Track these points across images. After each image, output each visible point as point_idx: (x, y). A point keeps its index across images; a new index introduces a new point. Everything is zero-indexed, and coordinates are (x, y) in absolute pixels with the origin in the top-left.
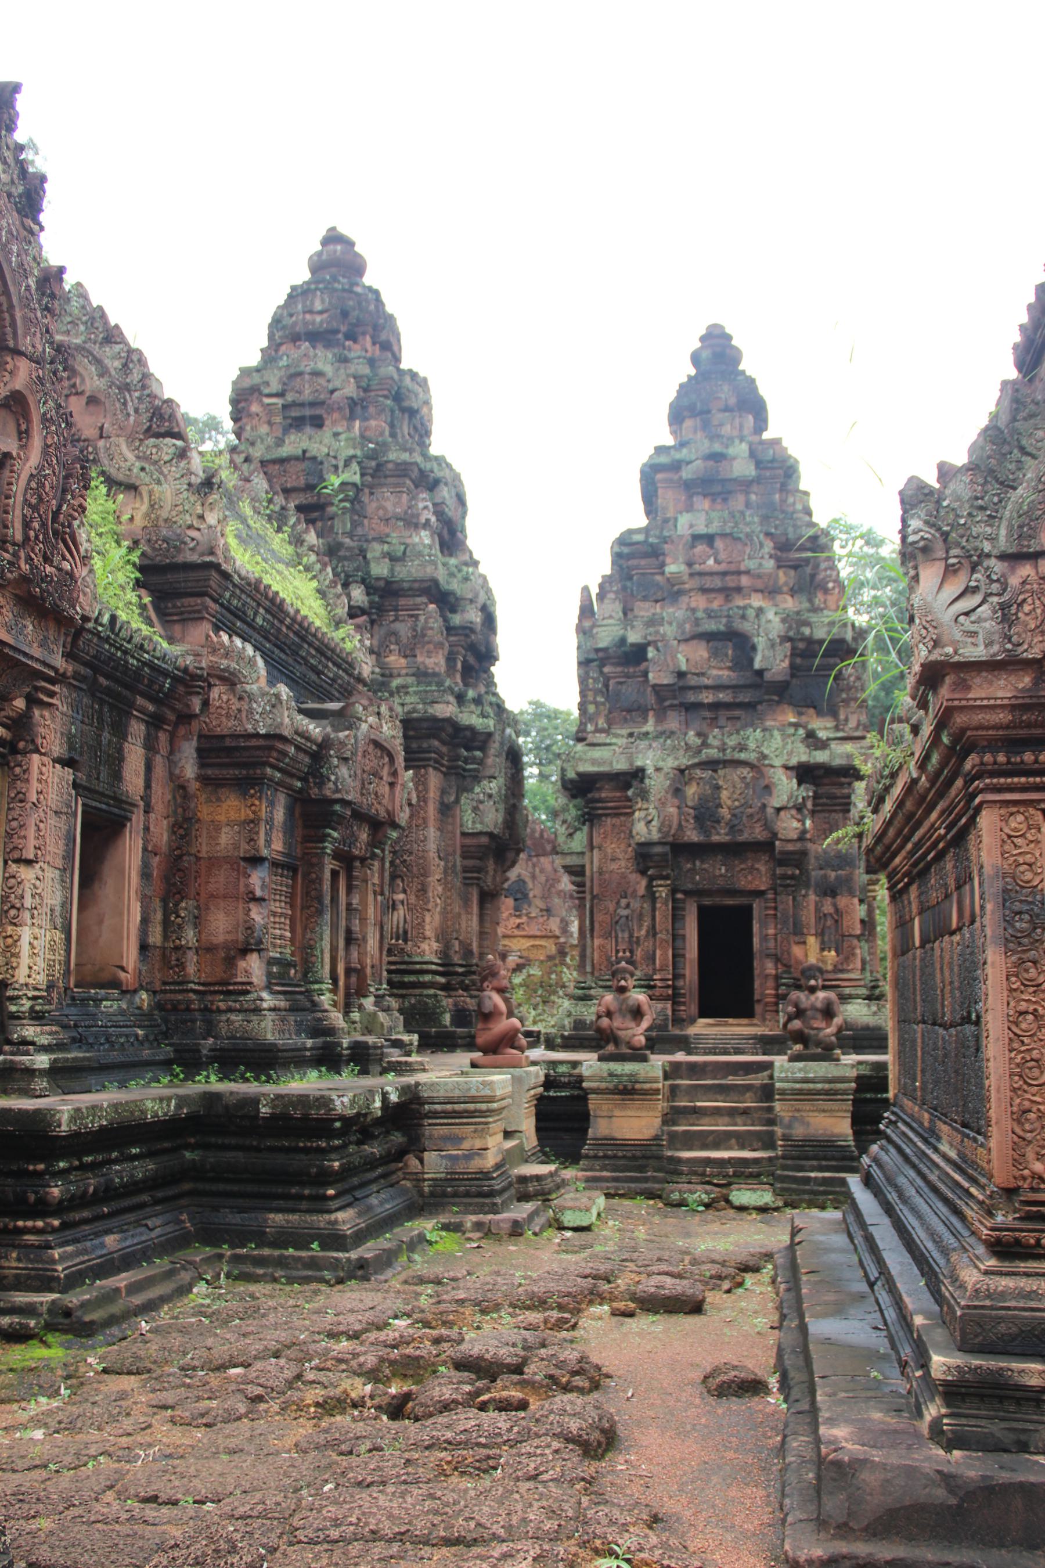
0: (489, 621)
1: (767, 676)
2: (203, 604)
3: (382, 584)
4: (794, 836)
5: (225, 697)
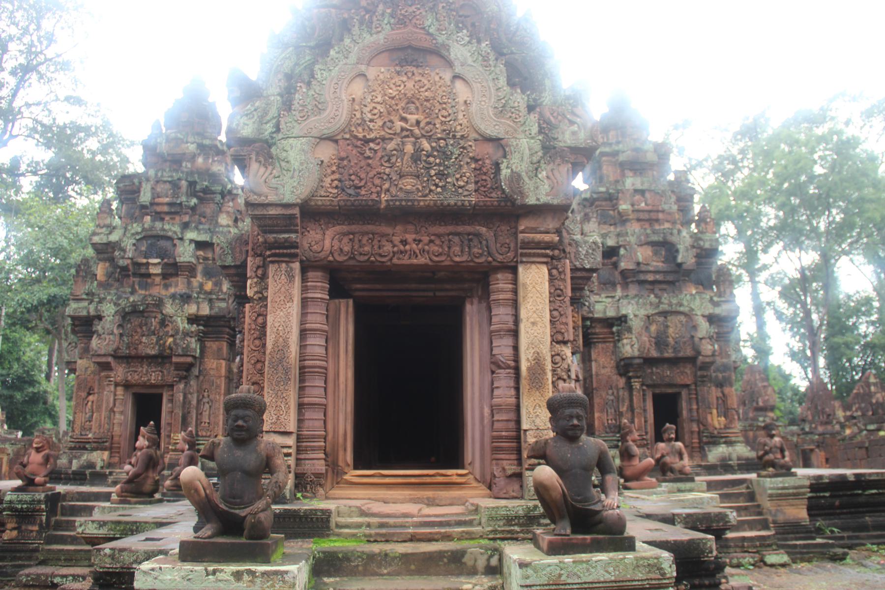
4: (710, 353)
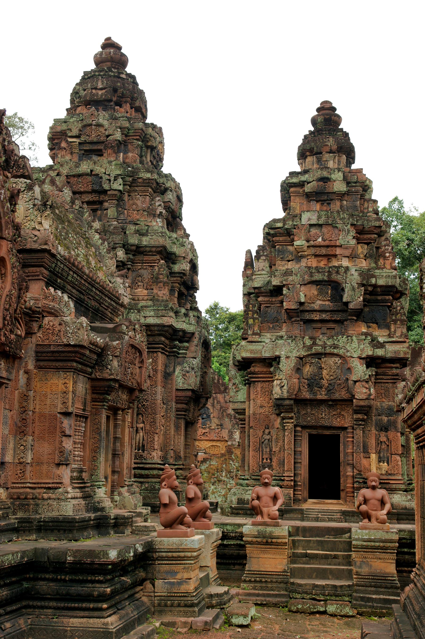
0: (194, 268)
1: (351, 306)
2: (40, 271)
3: (134, 248)
5: (51, 324)
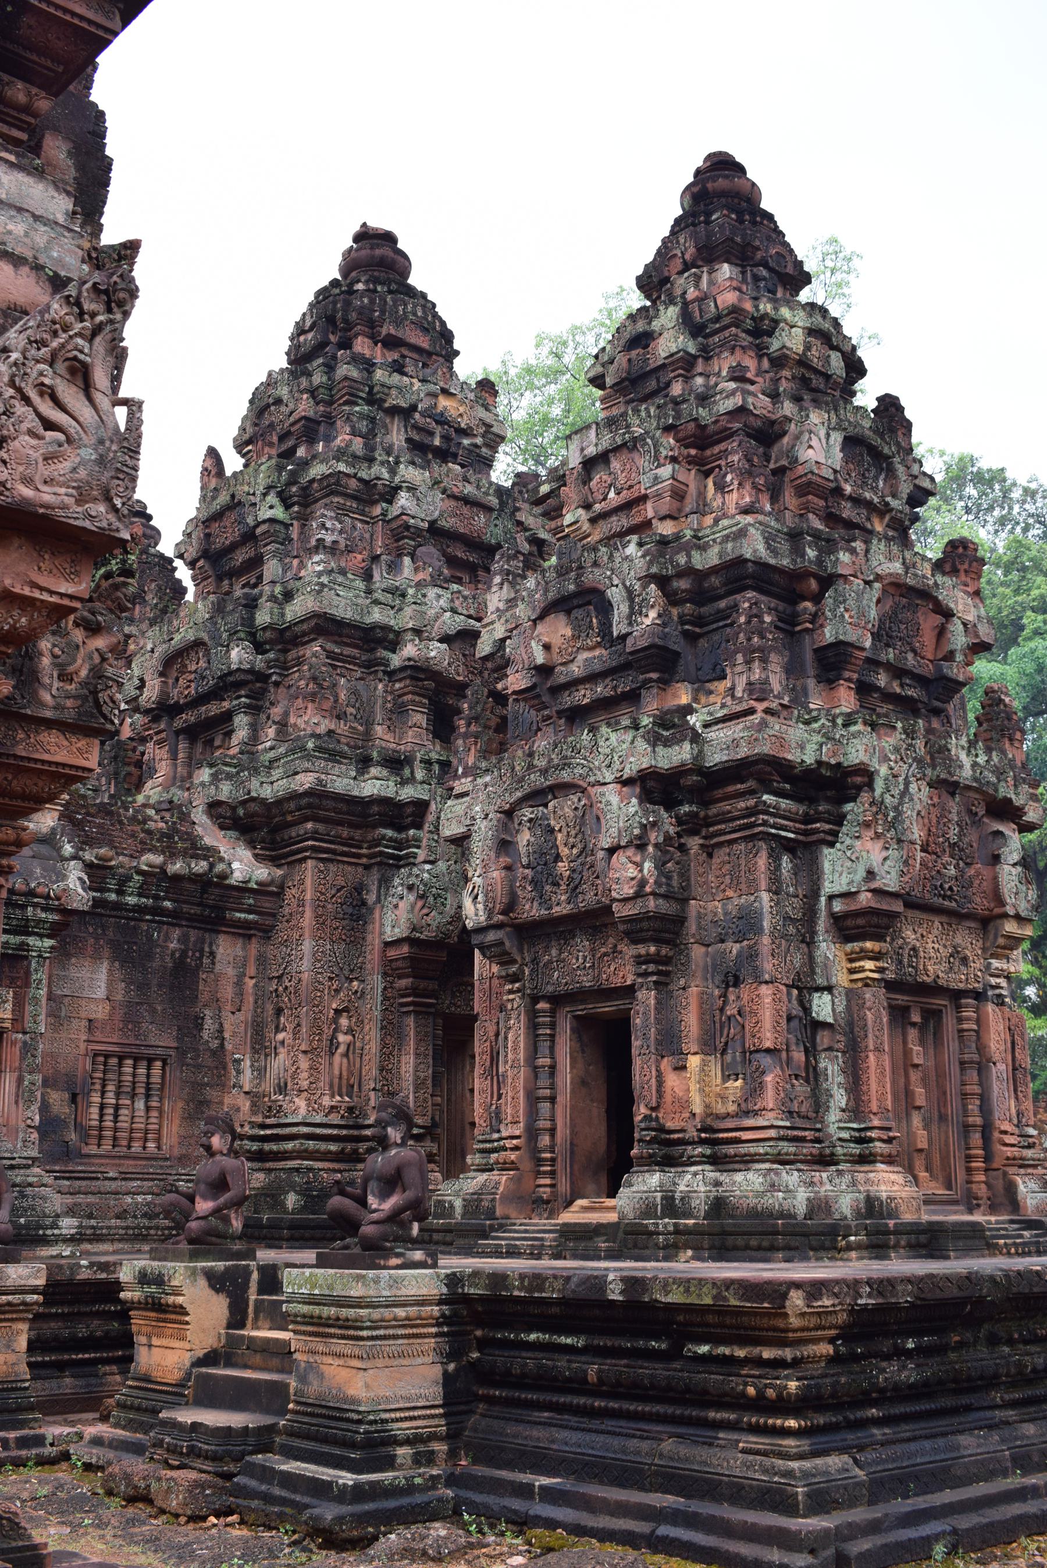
4: (629, 891)
